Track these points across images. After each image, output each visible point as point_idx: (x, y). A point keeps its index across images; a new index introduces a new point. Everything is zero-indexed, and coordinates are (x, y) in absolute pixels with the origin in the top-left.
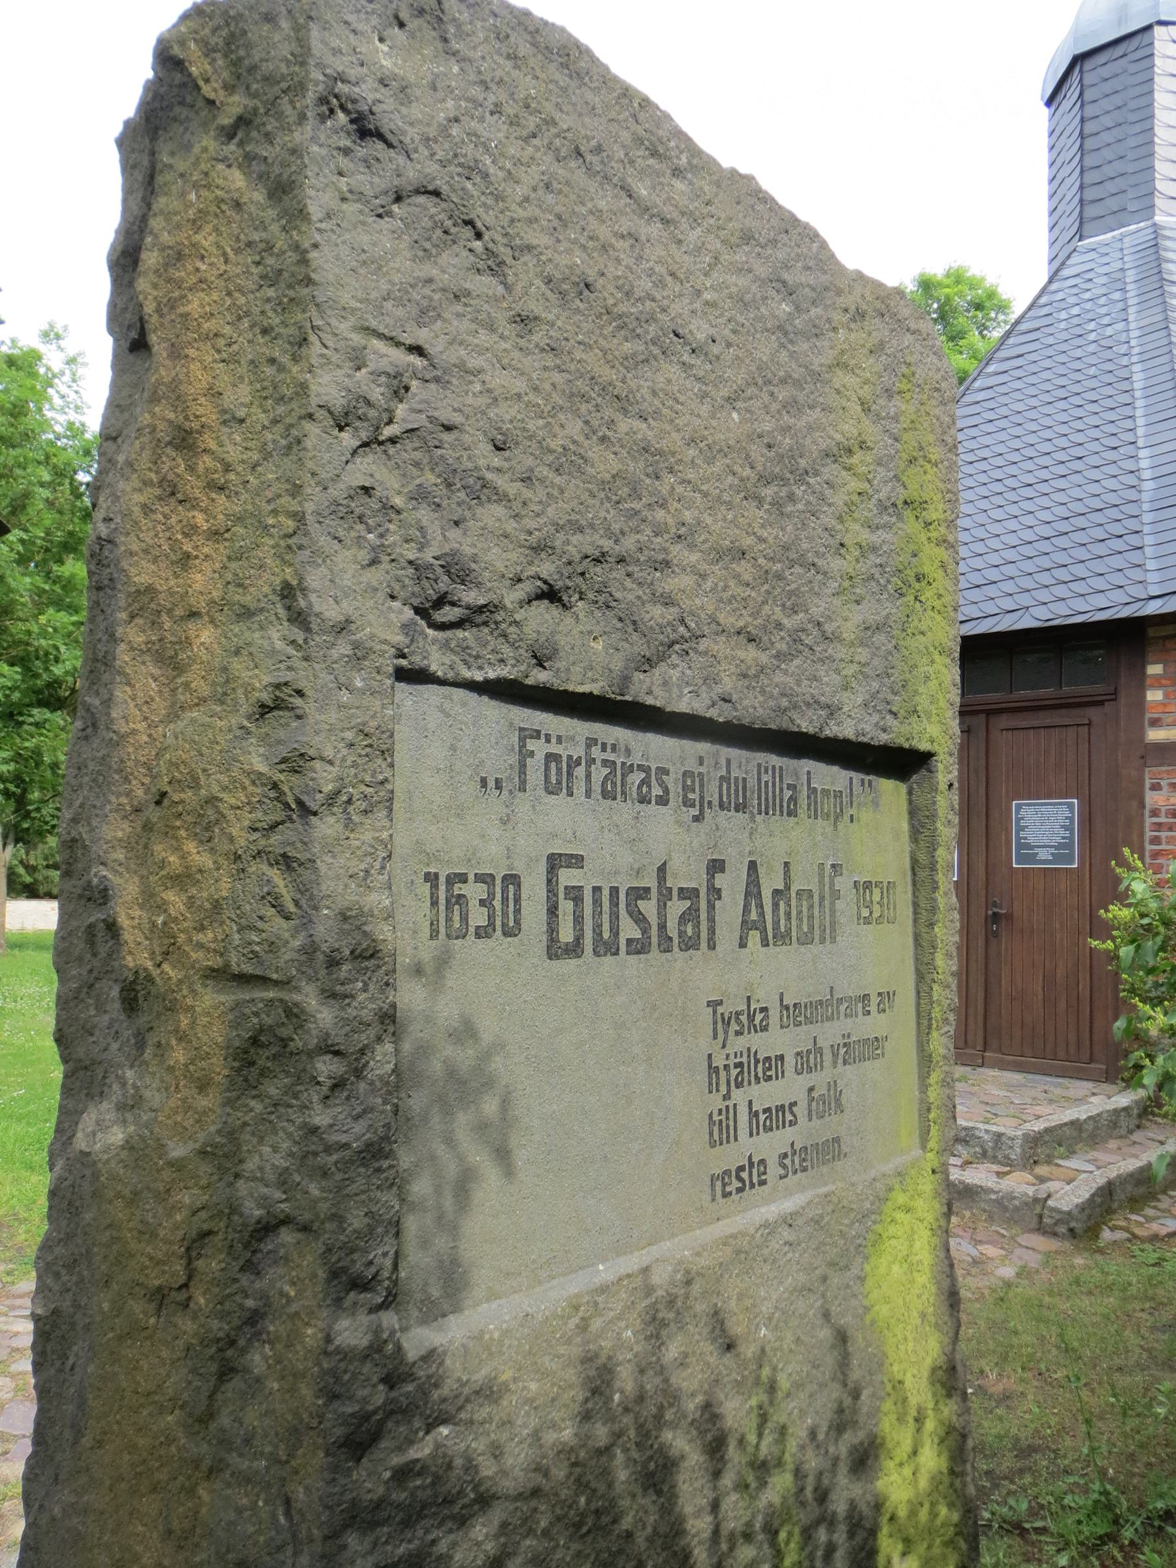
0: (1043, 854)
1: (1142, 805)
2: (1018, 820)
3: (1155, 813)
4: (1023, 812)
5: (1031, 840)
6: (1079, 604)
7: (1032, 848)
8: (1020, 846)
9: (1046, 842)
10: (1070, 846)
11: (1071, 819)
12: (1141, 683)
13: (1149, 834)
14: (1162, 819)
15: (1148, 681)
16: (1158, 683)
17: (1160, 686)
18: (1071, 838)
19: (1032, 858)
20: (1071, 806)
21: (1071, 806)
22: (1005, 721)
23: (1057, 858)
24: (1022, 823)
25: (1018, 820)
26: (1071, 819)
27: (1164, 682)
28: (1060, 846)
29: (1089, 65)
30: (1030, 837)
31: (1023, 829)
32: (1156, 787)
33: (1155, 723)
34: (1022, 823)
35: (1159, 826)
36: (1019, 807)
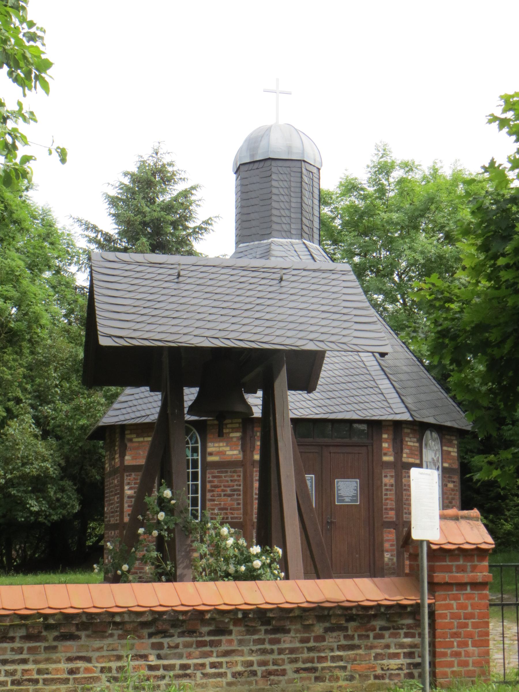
1: (382, 482)
2: (337, 487)
3: (386, 485)
4: (340, 483)
7: (343, 497)
8: (338, 496)
9: (348, 494)
10: (356, 496)
11: (357, 487)
12: (381, 441)
13: (384, 492)
14: (388, 487)
15: (383, 440)
16: (386, 441)
17: (386, 442)
18: (357, 494)
19: (343, 501)
20: (357, 482)
22: (332, 449)
23: (352, 501)
24: (339, 488)
25: (337, 487)
26: (357, 487)
27: (388, 441)
28: (353, 496)
29: (274, 163)
30: (342, 493)
31: (339, 490)
32: (386, 476)
33: (385, 454)
34: (339, 488)
35: (387, 490)
36: (338, 482)
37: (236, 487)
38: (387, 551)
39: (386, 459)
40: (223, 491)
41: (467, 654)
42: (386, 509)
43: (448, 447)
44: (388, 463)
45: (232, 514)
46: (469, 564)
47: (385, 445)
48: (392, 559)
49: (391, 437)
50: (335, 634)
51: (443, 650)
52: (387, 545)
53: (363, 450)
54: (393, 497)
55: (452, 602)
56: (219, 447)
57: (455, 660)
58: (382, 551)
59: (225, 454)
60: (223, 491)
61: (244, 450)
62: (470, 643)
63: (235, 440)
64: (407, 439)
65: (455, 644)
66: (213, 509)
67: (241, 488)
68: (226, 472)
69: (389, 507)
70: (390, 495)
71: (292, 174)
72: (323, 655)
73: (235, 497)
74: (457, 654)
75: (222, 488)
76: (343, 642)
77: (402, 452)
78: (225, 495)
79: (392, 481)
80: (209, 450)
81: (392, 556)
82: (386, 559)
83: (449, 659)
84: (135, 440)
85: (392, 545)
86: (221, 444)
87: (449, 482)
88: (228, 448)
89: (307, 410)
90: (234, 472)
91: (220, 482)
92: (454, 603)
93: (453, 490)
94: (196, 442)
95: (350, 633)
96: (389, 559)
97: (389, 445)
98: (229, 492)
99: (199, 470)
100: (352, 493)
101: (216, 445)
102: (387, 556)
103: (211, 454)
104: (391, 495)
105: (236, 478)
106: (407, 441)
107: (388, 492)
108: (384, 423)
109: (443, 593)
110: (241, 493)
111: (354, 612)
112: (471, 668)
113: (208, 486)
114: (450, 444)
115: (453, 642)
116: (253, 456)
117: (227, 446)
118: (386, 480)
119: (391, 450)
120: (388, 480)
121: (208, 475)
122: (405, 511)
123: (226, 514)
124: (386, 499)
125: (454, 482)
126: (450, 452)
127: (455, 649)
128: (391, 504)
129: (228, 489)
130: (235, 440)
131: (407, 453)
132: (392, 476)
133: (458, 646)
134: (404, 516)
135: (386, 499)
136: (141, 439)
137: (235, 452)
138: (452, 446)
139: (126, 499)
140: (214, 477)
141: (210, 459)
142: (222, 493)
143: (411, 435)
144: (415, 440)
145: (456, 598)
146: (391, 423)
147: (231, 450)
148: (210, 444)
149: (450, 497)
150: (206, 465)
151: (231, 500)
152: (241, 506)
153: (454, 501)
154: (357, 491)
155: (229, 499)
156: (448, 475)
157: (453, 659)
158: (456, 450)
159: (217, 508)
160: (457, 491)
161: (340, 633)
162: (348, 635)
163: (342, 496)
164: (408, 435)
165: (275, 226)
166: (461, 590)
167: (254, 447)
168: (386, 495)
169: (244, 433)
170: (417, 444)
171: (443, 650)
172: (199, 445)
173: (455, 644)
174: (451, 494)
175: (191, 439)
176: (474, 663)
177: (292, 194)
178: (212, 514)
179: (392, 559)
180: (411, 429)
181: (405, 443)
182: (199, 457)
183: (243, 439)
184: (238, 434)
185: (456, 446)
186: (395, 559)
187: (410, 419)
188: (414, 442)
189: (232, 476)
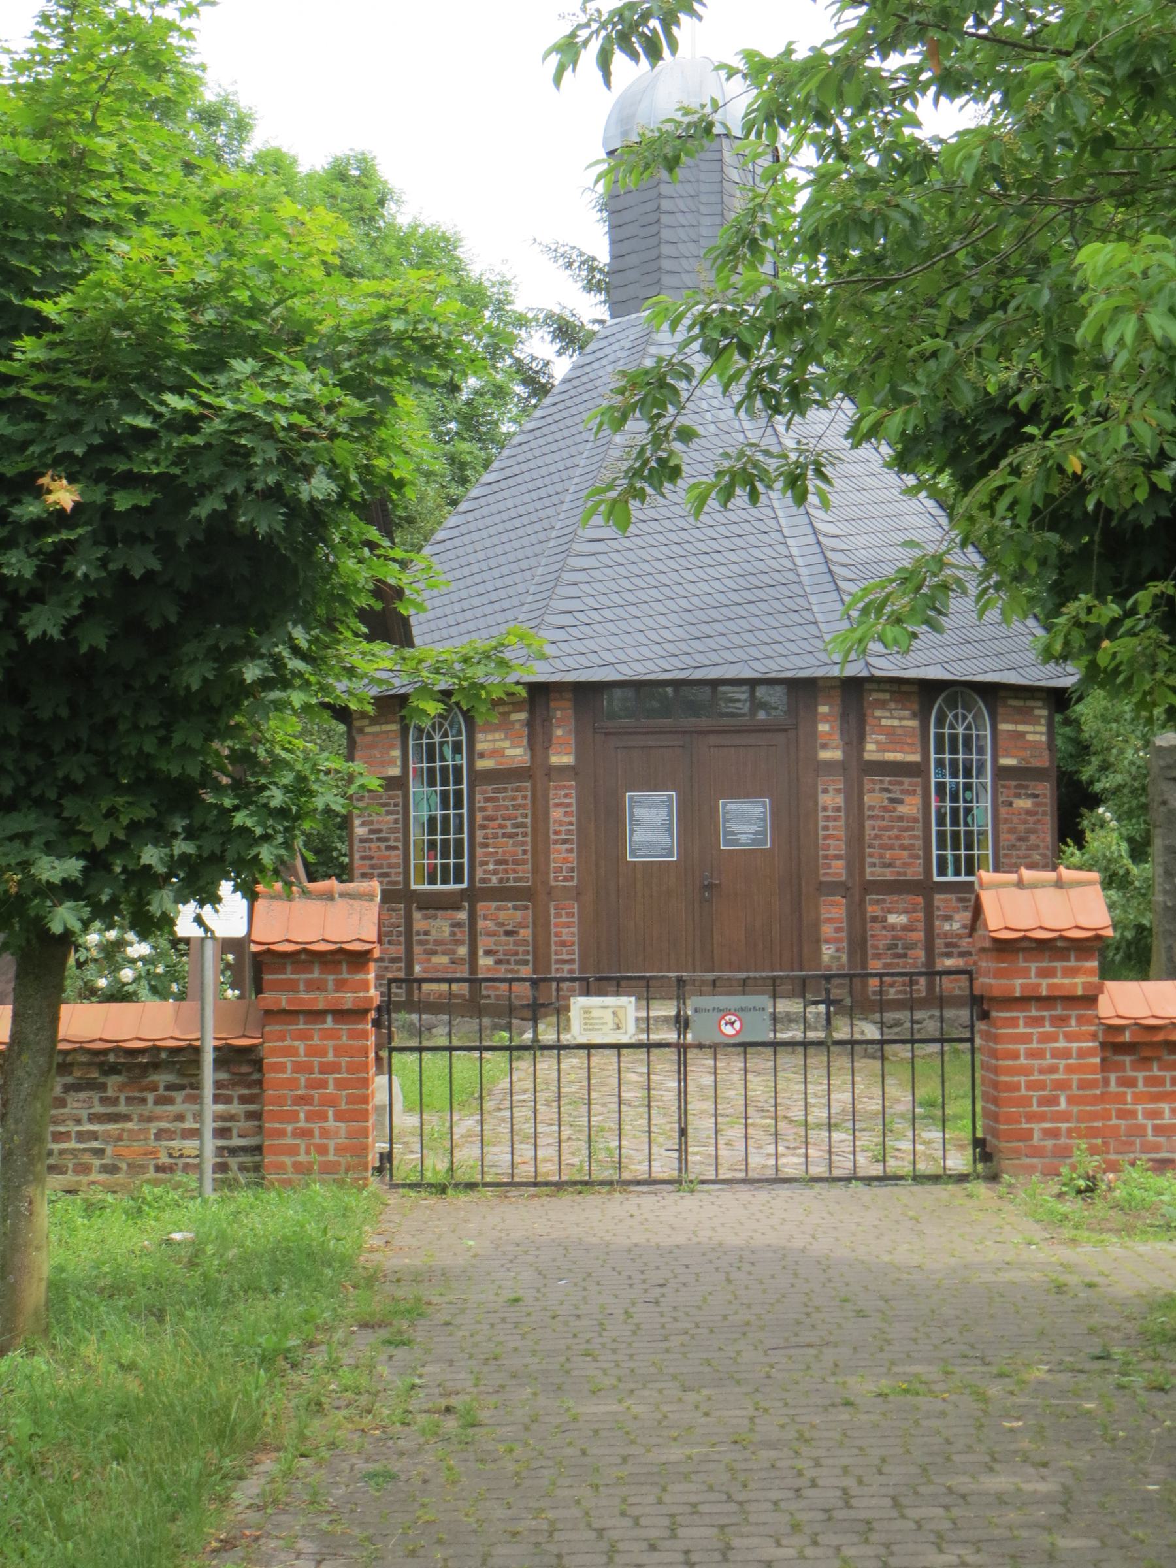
0: (744, 839)
1: (816, 803)
3: (825, 809)
4: (728, 808)
5: (735, 829)
6: (783, 662)
8: (726, 833)
10: (764, 833)
12: (814, 719)
13: (821, 823)
17: (827, 721)
19: (736, 842)
20: (764, 804)
21: (764, 804)
22: (713, 740)
23: (754, 841)
28: (757, 833)
30: (734, 826)
31: (728, 820)
32: (825, 791)
33: (825, 746)
35: (827, 818)
36: (725, 805)
37: (520, 820)
38: (828, 941)
39: (824, 755)
40: (501, 826)
41: (325, 1134)
42: (826, 857)
43: (1016, 723)
44: (830, 765)
45: (515, 871)
46: (331, 977)
47: (823, 728)
48: (839, 958)
49: (837, 710)
50: (83, 1095)
51: (277, 1125)
52: (827, 930)
53: (780, 738)
54: (842, 833)
55: (296, 1043)
56: (494, 740)
57: (302, 1144)
58: (817, 942)
59: (503, 756)
60: (501, 826)
61: (531, 746)
62: (330, 1114)
63: (517, 726)
64: (878, 713)
65: (302, 1115)
66: (487, 863)
67: (528, 820)
68: (505, 790)
69: (832, 852)
70: (835, 828)
71: (703, 166)
72: (62, 1129)
73: (520, 838)
74: (306, 1134)
75: (500, 821)
76: (99, 1109)
77: (861, 739)
78: (504, 835)
79: (840, 800)
80: (480, 747)
81: (837, 950)
82: (825, 959)
83: (289, 1141)
84: (368, 730)
85: (838, 930)
86: (497, 736)
87: (1018, 796)
88: (507, 744)
89: (649, 664)
90: (517, 790)
91: (497, 809)
92: (301, 1046)
93: (1029, 812)
94: (459, 733)
95: (110, 1093)
96: (832, 957)
97: (832, 728)
98: (509, 830)
99: (465, 787)
100: (756, 825)
101: (490, 737)
102: (827, 951)
103: (482, 755)
104: (838, 828)
105: (520, 801)
106: (880, 718)
107: (831, 824)
108: (820, 683)
109: (278, 1027)
110: (529, 830)
111: (112, 1058)
112: (331, 1157)
113: (479, 816)
114: (1025, 715)
115: (297, 1112)
116: (547, 757)
117: (506, 738)
118: (824, 799)
119: (837, 736)
120: (831, 798)
121: (478, 797)
122: (869, 860)
123: (506, 871)
124: (826, 838)
125: (1036, 796)
126: (1022, 735)
127: (302, 1124)
128: (837, 847)
129: (509, 823)
130: (517, 726)
131: (877, 742)
132: (838, 791)
133: (308, 1119)
134: (868, 870)
135: (826, 838)
136: (376, 729)
137: (519, 751)
138: (1035, 721)
139: (357, 844)
140: (487, 800)
141: (482, 764)
142: (500, 831)
143: (893, 705)
144: (907, 713)
145: (304, 1036)
146: (838, 683)
147: (513, 747)
148: (480, 736)
149: (1022, 827)
150: (477, 778)
151: (515, 844)
152: (528, 856)
153: (1033, 837)
154: (764, 820)
155: (511, 841)
156: (1013, 783)
157: (297, 1142)
158: (1043, 729)
159: (492, 860)
160: (1044, 813)
161: (90, 1094)
162: (107, 1098)
163: (733, 833)
164: (882, 704)
165: (667, 280)
166: (315, 1023)
167: (550, 740)
168: (826, 828)
169: (532, 712)
170: (914, 723)
171: (277, 1125)
172: (464, 738)
173: (302, 1115)
174: (1025, 822)
175: (451, 726)
176: (339, 1150)
177: (703, 209)
178: (485, 872)
179: (839, 958)
180: (892, 692)
181: (870, 720)
182: (464, 762)
183: (530, 724)
184: (523, 716)
185: (1043, 721)
186: (844, 958)
187: (865, 674)
188: (901, 719)
189: (514, 798)
